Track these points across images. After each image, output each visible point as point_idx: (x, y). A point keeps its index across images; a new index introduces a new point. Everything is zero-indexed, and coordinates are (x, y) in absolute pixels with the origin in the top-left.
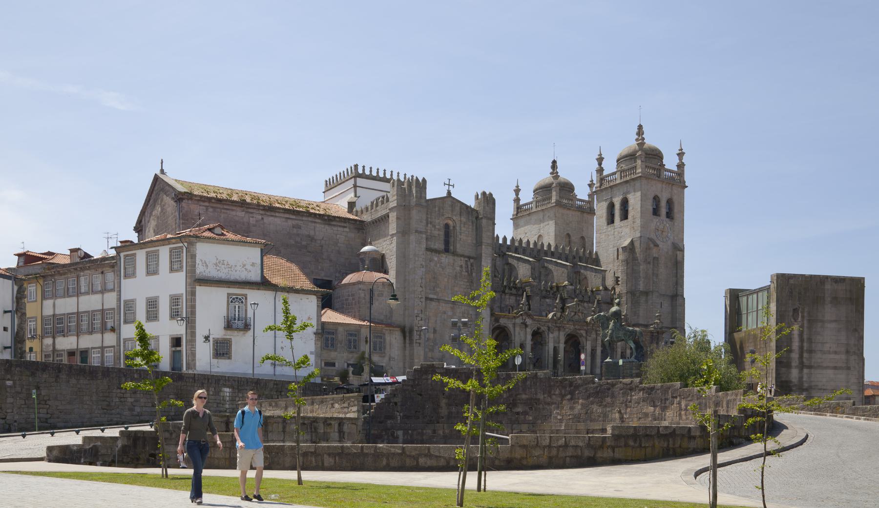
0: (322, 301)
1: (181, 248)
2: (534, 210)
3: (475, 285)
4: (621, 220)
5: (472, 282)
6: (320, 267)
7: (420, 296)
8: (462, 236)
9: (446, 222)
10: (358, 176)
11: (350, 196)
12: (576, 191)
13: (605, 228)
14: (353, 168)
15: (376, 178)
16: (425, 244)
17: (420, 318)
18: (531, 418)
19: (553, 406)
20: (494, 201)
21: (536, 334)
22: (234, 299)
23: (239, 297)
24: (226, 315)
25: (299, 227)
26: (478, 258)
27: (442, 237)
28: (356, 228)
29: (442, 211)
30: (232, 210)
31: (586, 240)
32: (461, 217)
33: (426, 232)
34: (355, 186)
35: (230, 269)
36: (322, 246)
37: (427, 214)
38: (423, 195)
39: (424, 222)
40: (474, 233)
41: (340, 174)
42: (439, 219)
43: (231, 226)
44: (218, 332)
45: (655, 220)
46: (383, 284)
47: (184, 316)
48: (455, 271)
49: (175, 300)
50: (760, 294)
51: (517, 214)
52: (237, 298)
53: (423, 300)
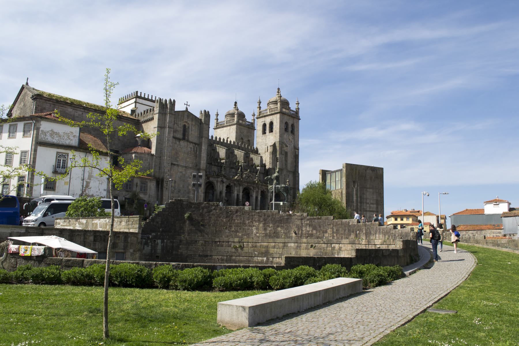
0: (113, 160)
1: (31, 123)
2: (225, 125)
3: (198, 158)
4: (270, 132)
5: (196, 157)
8: (192, 132)
9: (184, 124)
10: (137, 97)
11: (133, 106)
12: (246, 117)
13: (261, 136)
14: (135, 93)
15: (148, 99)
18: (240, 235)
19: (254, 227)
20: (209, 115)
21: (228, 187)
22: (60, 155)
23: (64, 154)
24: (54, 165)
26: (199, 145)
27: (182, 132)
29: (182, 118)
30: (65, 107)
31: (251, 142)
32: (192, 122)
33: (173, 128)
34: (136, 102)
35: (60, 138)
37: (175, 119)
38: (173, 108)
39: (173, 122)
40: (199, 131)
41: (128, 95)
44: (49, 174)
45: (286, 134)
46: (148, 154)
47: (29, 163)
49: (24, 153)
50: (337, 173)
52: (62, 155)
53: (170, 164)
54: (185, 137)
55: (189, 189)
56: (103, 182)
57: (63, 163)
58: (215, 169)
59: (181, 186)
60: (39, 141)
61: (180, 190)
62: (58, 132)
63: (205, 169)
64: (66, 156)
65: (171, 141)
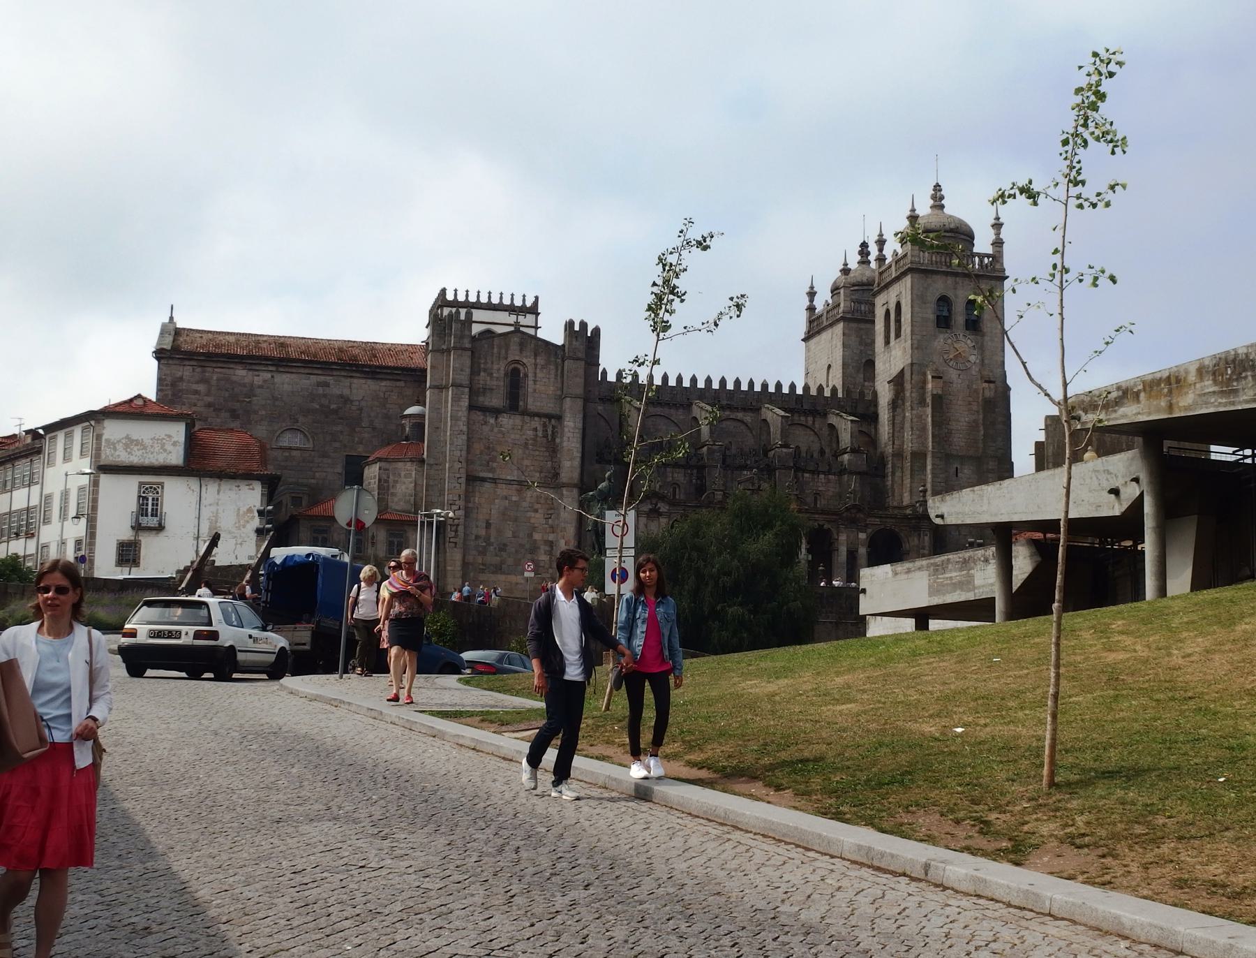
0: (269, 488)
6: (356, 439)
7: (458, 475)
9: (513, 366)
16: (467, 400)
17: (457, 507)
22: (147, 489)
25: (326, 385)
28: (415, 381)
32: (536, 359)
36: (361, 409)
38: (467, 333)
42: (498, 364)
43: (227, 391)
45: (942, 336)
48: (524, 437)
51: (809, 332)
52: (151, 488)
53: (463, 480)
54: (514, 402)
55: (536, 540)
56: (246, 539)
57: (153, 505)
58: (676, 475)
59: (509, 534)
60: (102, 463)
61: (505, 545)
62: (140, 439)
63: (576, 481)
64: (157, 488)
65: (464, 419)
